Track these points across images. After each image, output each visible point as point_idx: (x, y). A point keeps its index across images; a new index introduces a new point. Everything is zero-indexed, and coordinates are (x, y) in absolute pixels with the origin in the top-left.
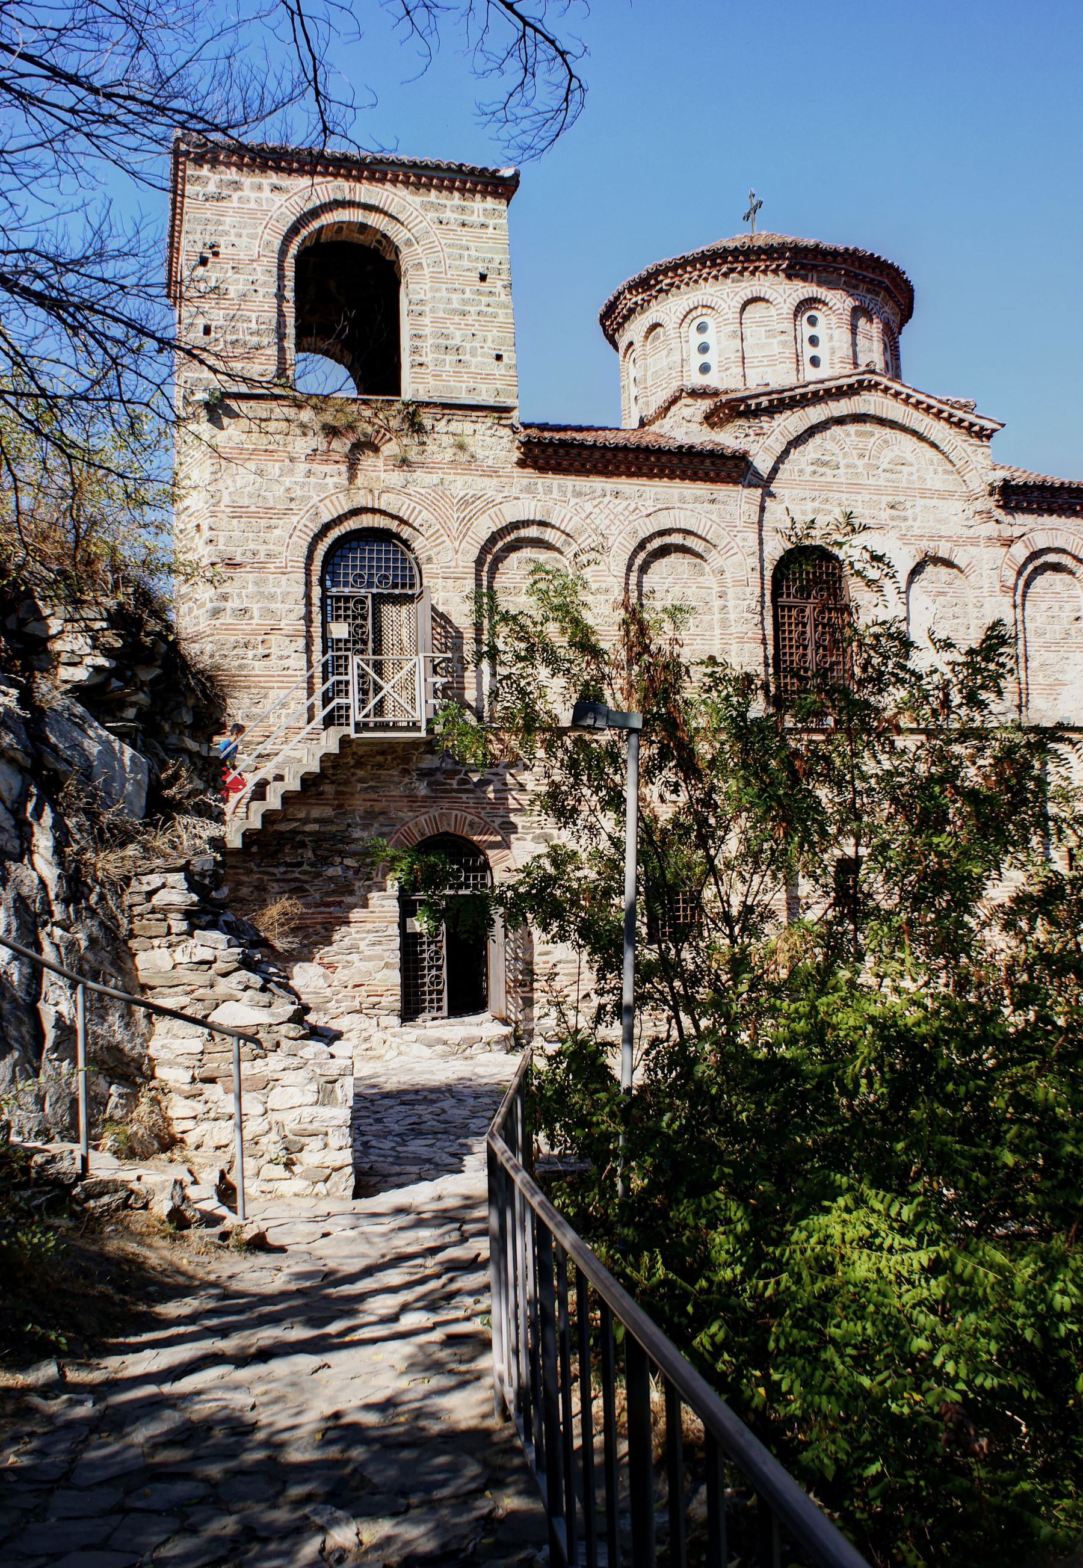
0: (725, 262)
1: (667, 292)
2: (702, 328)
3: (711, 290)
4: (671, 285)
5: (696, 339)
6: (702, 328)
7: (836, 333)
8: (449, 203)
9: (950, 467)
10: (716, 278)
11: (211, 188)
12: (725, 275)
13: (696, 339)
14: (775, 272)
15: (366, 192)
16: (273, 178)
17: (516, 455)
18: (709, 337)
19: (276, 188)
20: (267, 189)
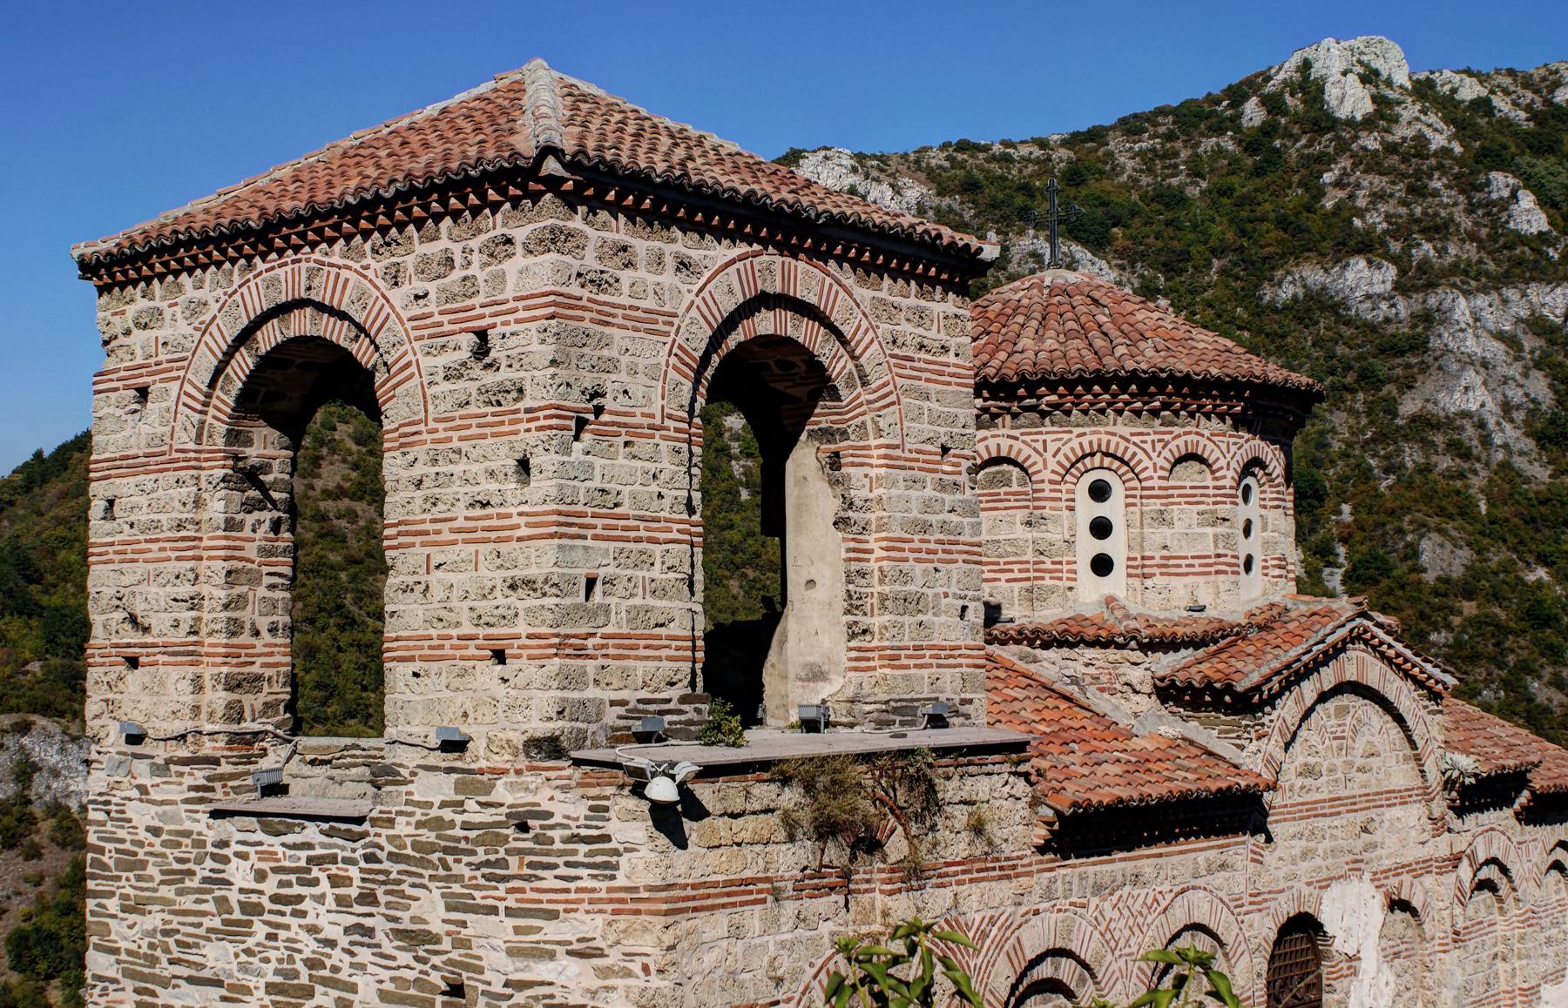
0: (1162, 392)
1: (1043, 414)
2: (1099, 492)
3: (1126, 431)
4: (1056, 406)
5: (1089, 510)
6: (1099, 492)
7: (1272, 515)
8: (904, 302)
9: (1409, 752)
10: (1138, 413)
11: (590, 261)
12: (1155, 413)
13: (1089, 510)
14: (1221, 417)
15: (806, 279)
16: (681, 244)
17: (1040, 834)
18: (1112, 509)
19: (683, 265)
20: (670, 262)
